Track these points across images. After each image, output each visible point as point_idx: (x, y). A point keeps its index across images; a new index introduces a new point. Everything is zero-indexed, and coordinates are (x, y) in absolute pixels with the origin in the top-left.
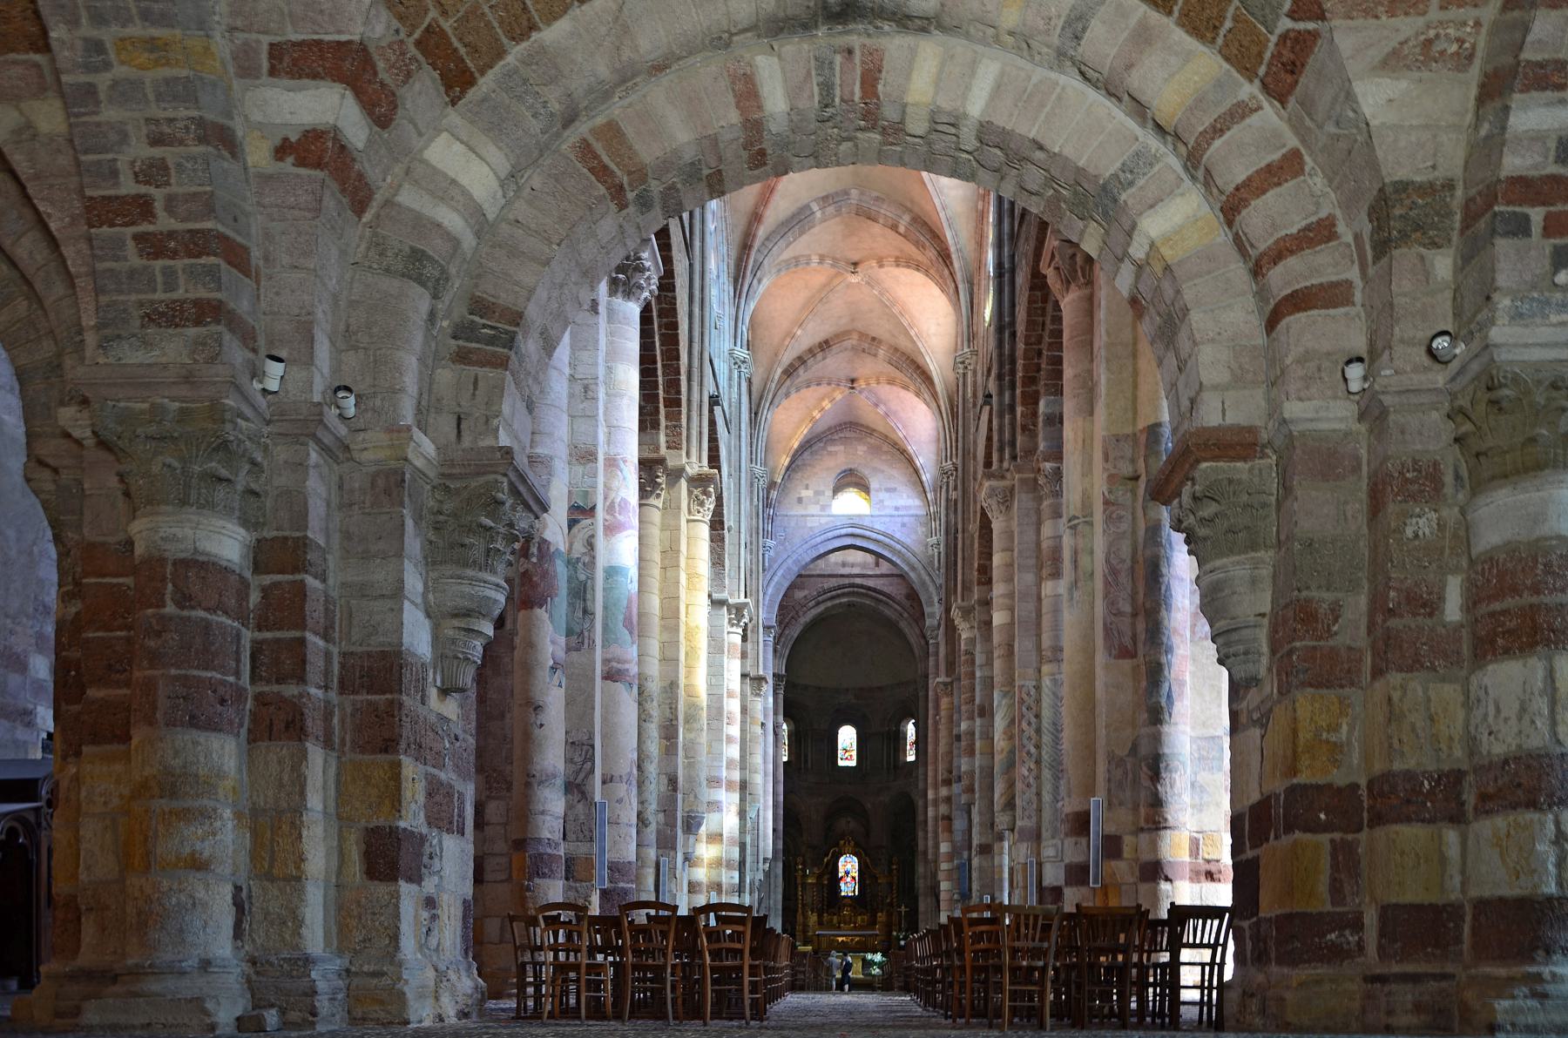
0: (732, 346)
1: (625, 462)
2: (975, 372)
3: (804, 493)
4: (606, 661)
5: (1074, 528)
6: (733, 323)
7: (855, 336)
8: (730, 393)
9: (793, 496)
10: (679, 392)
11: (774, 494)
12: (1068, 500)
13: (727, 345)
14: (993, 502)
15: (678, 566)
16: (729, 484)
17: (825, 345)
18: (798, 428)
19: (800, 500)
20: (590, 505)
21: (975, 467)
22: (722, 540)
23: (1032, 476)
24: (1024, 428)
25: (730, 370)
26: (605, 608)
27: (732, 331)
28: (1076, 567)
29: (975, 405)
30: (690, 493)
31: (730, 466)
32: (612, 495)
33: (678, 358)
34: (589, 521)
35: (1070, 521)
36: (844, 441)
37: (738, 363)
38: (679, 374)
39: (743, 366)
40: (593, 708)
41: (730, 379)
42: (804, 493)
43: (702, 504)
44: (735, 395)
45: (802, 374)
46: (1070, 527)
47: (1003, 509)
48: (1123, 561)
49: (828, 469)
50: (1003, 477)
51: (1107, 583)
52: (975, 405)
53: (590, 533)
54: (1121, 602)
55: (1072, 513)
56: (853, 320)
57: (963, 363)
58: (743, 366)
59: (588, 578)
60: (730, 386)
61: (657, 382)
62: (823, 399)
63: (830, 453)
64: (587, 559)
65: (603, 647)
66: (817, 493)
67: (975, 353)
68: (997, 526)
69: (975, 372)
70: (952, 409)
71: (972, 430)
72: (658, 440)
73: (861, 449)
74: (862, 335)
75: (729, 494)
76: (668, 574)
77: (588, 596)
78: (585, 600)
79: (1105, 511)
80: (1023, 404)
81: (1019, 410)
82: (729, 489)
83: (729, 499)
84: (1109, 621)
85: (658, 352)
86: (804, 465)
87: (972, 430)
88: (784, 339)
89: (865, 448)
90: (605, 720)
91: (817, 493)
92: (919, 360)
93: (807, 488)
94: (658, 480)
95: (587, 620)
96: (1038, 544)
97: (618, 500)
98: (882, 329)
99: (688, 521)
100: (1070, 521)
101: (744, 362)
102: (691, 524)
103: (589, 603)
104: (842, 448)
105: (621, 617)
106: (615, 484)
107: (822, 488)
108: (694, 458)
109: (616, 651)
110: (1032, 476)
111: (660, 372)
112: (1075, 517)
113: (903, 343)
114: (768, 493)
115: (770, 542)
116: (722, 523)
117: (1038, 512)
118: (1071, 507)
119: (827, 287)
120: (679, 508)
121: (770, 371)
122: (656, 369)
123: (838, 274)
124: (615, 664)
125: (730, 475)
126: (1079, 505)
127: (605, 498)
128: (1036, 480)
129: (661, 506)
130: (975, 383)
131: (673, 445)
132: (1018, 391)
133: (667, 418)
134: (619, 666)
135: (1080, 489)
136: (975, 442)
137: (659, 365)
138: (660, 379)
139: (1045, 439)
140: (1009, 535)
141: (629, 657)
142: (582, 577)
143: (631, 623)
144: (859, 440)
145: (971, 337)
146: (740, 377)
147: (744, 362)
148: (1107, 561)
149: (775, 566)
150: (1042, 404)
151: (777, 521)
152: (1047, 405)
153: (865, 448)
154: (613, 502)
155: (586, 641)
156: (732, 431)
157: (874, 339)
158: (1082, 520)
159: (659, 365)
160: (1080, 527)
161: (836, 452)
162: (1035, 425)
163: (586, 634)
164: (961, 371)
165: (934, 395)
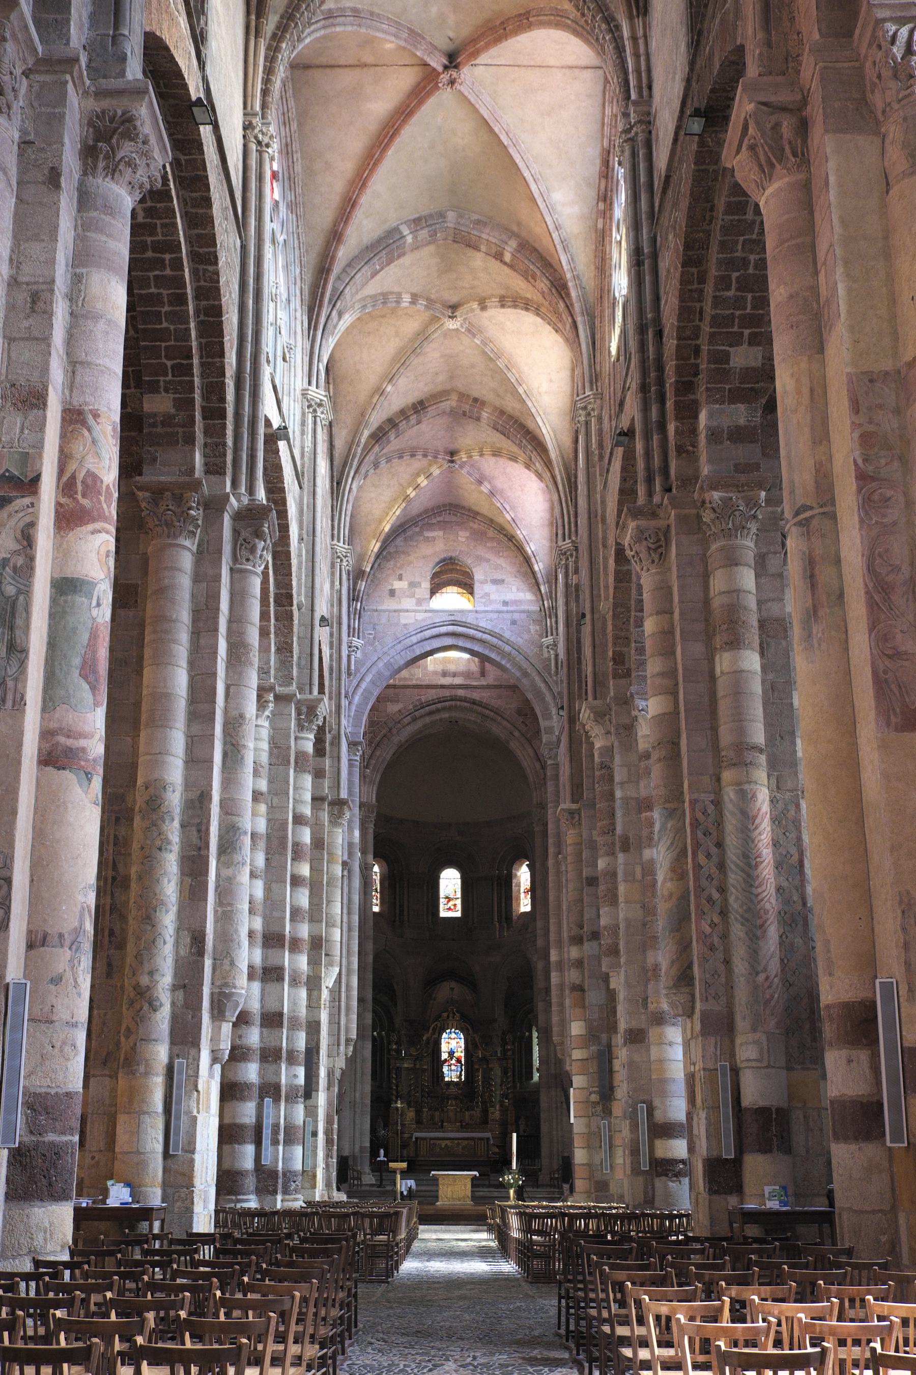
0: (306, 386)
1: (96, 416)
2: (600, 419)
3: (397, 585)
4: (46, 734)
5: (805, 524)
6: (307, 359)
7: (454, 397)
8: (302, 441)
10: (223, 400)
11: (362, 585)
12: (792, 482)
13: (300, 382)
14: (642, 548)
15: (216, 630)
16: (300, 550)
17: (419, 407)
18: (390, 508)
19: (392, 593)
20: (31, 475)
21: (604, 532)
22: (290, 617)
23: (694, 511)
24: (680, 450)
25: (303, 414)
26: (52, 644)
27: (306, 368)
28: (813, 586)
29: (601, 458)
30: (236, 532)
31: (301, 528)
32: (72, 467)
33: (222, 354)
34: (27, 501)
35: (797, 514)
36: (444, 525)
37: (312, 406)
38: (223, 375)
39: (319, 410)
40: (14, 812)
41: (303, 423)
42: (397, 585)
43: (253, 550)
44: (309, 443)
45: (394, 443)
46: (799, 524)
47: (656, 557)
48: (897, 569)
50: (654, 515)
51: (872, 606)
52: (601, 458)
53: (28, 519)
54: (899, 636)
55: (800, 501)
56: (452, 378)
57: (585, 408)
58: (319, 410)
59: (19, 592)
60: (303, 433)
61: (192, 382)
62: (418, 475)
64: (20, 561)
65: (44, 709)
66: (412, 585)
67: (600, 396)
68: (647, 580)
69: (600, 419)
70: (569, 480)
71: (599, 488)
72: (193, 459)
73: (463, 535)
74: (463, 396)
75: (300, 563)
76: (202, 642)
77: (19, 622)
78: (12, 628)
79: (859, 490)
80: (677, 418)
81: (671, 428)
82: (300, 555)
83: (300, 568)
84: (881, 667)
85: (194, 344)
86: (396, 552)
87: (599, 488)
88: (372, 396)
89: (467, 534)
90: (40, 834)
91: (412, 585)
92: (530, 425)
93: (400, 578)
94: (192, 512)
95: (15, 663)
96: (707, 602)
97: (81, 476)
98: (483, 389)
99: (231, 569)
100: (797, 514)
101: (320, 405)
102: (236, 576)
103: (18, 632)
104: (441, 533)
105: (77, 661)
106: (78, 448)
107: (417, 579)
108: (243, 490)
109: (65, 716)
110: (694, 511)
111: (196, 371)
112: (805, 508)
113: (510, 405)
114: (355, 584)
115: (357, 642)
116: (290, 596)
117: (704, 559)
118: (799, 492)
119: (422, 337)
120: (220, 552)
121: (355, 433)
122: (192, 365)
123: (435, 319)
124: (62, 739)
125: (301, 539)
126: (811, 487)
127: (61, 471)
128: (699, 517)
129: (194, 548)
130: (600, 432)
131: (215, 468)
132: (669, 404)
133: (207, 432)
134: (70, 742)
135: (811, 462)
136: (603, 502)
137: (196, 361)
138: (197, 380)
139: (710, 461)
140: (664, 590)
141: (87, 728)
142: (10, 590)
143: (95, 672)
145: (595, 378)
146: (315, 423)
147: (320, 405)
148: (870, 568)
149: (363, 670)
150: (703, 417)
151: (366, 616)
152: (711, 416)
153: (467, 534)
154: (73, 478)
155: (10, 697)
156: (305, 486)
157: (476, 400)
158: (816, 511)
159: (196, 361)
160: (815, 522)
162: (694, 445)
163: (10, 684)
164: (583, 419)
165: (548, 464)
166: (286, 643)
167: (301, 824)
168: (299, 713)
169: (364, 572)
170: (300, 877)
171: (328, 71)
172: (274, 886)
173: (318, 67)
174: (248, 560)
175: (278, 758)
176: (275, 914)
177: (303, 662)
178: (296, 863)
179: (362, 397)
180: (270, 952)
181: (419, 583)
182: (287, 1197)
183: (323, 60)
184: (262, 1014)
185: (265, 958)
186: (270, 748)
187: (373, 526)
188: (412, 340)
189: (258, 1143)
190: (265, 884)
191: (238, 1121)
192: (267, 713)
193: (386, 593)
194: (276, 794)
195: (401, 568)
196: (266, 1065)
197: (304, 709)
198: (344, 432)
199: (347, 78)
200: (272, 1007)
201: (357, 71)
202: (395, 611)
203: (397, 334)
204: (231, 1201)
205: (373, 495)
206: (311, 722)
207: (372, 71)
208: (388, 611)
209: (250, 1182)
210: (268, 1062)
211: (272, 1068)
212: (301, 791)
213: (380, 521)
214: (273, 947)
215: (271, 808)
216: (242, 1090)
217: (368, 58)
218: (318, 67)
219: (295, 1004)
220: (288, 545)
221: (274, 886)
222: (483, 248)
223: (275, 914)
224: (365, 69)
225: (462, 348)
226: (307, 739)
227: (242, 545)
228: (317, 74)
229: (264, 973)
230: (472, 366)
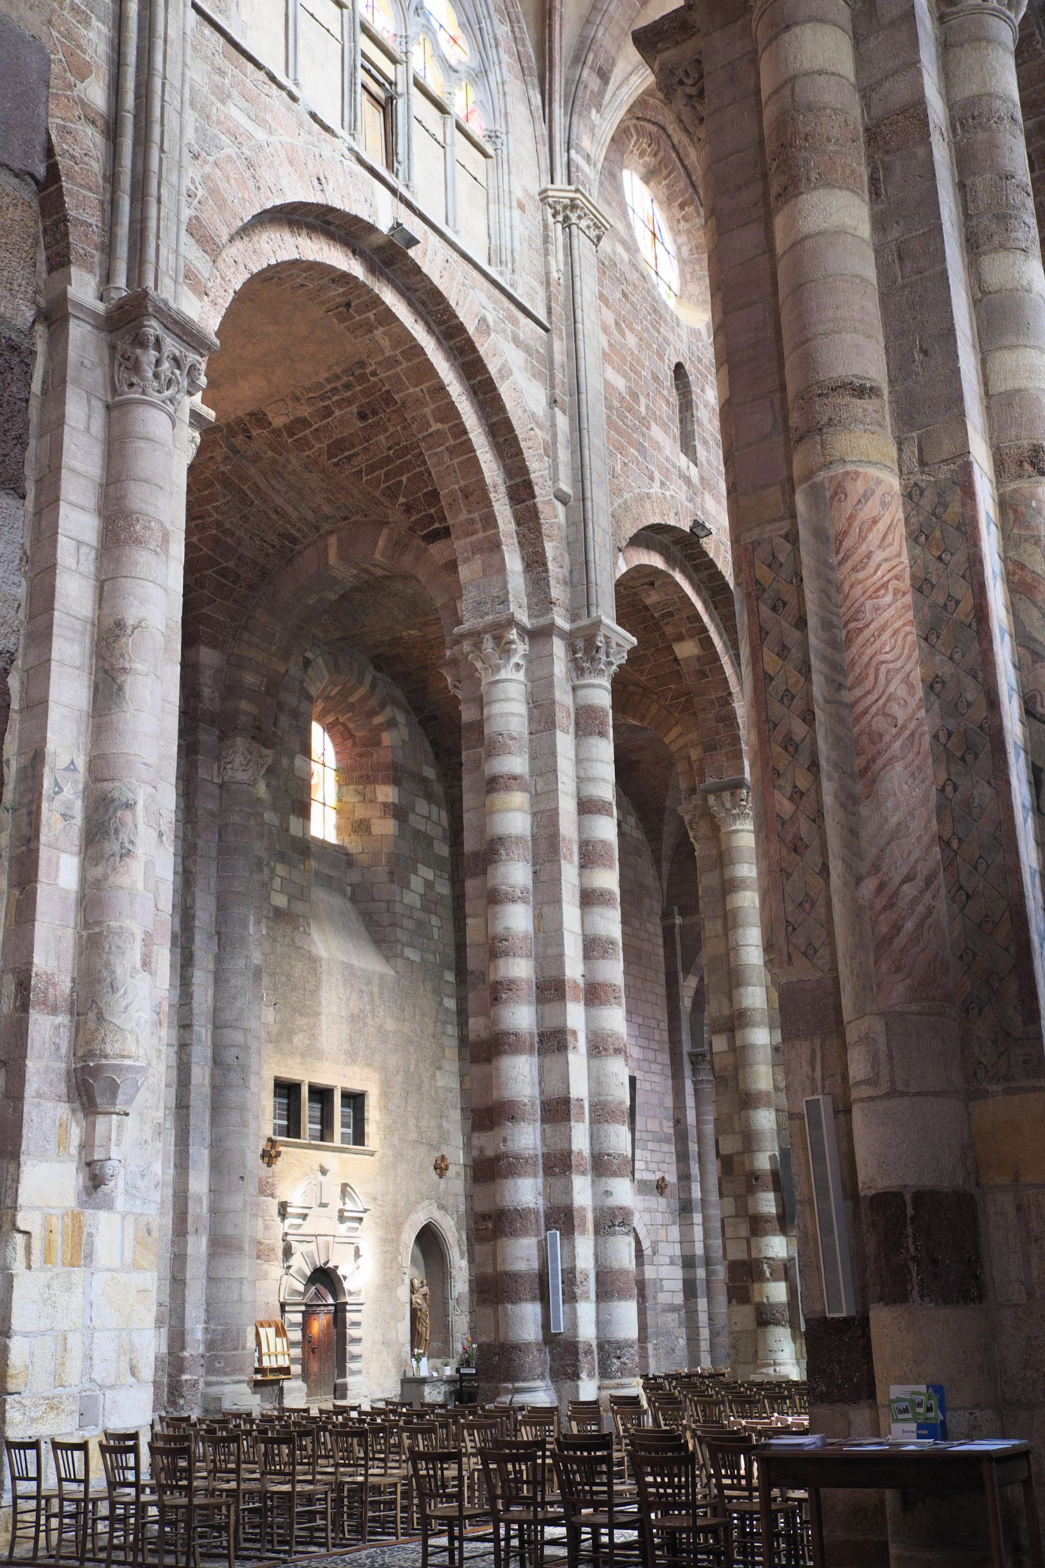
25: (546, 227)
41: (546, 239)
44: (557, 264)
101: (573, 207)
116: (528, 485)
166: (536, 553)
167: (591, 812)
168: (572, 649)
170: (594, 891)
172: (546, 910)
174: (131, 385)
175: (539, 721)
176: (551, 951)
177: (576, 576)
178: (587, 872)
180: (547, 1007)
182: (607, 1382)
184: (542, 1103)
185: (540, 1019)
186: (530, 710)
189: (544, 1298)
190: (535, 909)
191: (509, 1268)
192: (516, 659)
194: (541, 775)
196: (552, 1180)
197: (580, 644)
200: (555, 1090)
204: (508, 1391)
206: (593, 660)
209: (537, 1360)
210: (553, 1174)
211: (559, 1183)
212: (586, 764)
214: (550, 1001)
215: (536, 797)
216: (513, 1220)
219: (599, 1083)
220: (503, 409)
221: (546, 910)
223: (551, 951)
226: (600, 686)
227: (120, 365)
229: (541, 1041)
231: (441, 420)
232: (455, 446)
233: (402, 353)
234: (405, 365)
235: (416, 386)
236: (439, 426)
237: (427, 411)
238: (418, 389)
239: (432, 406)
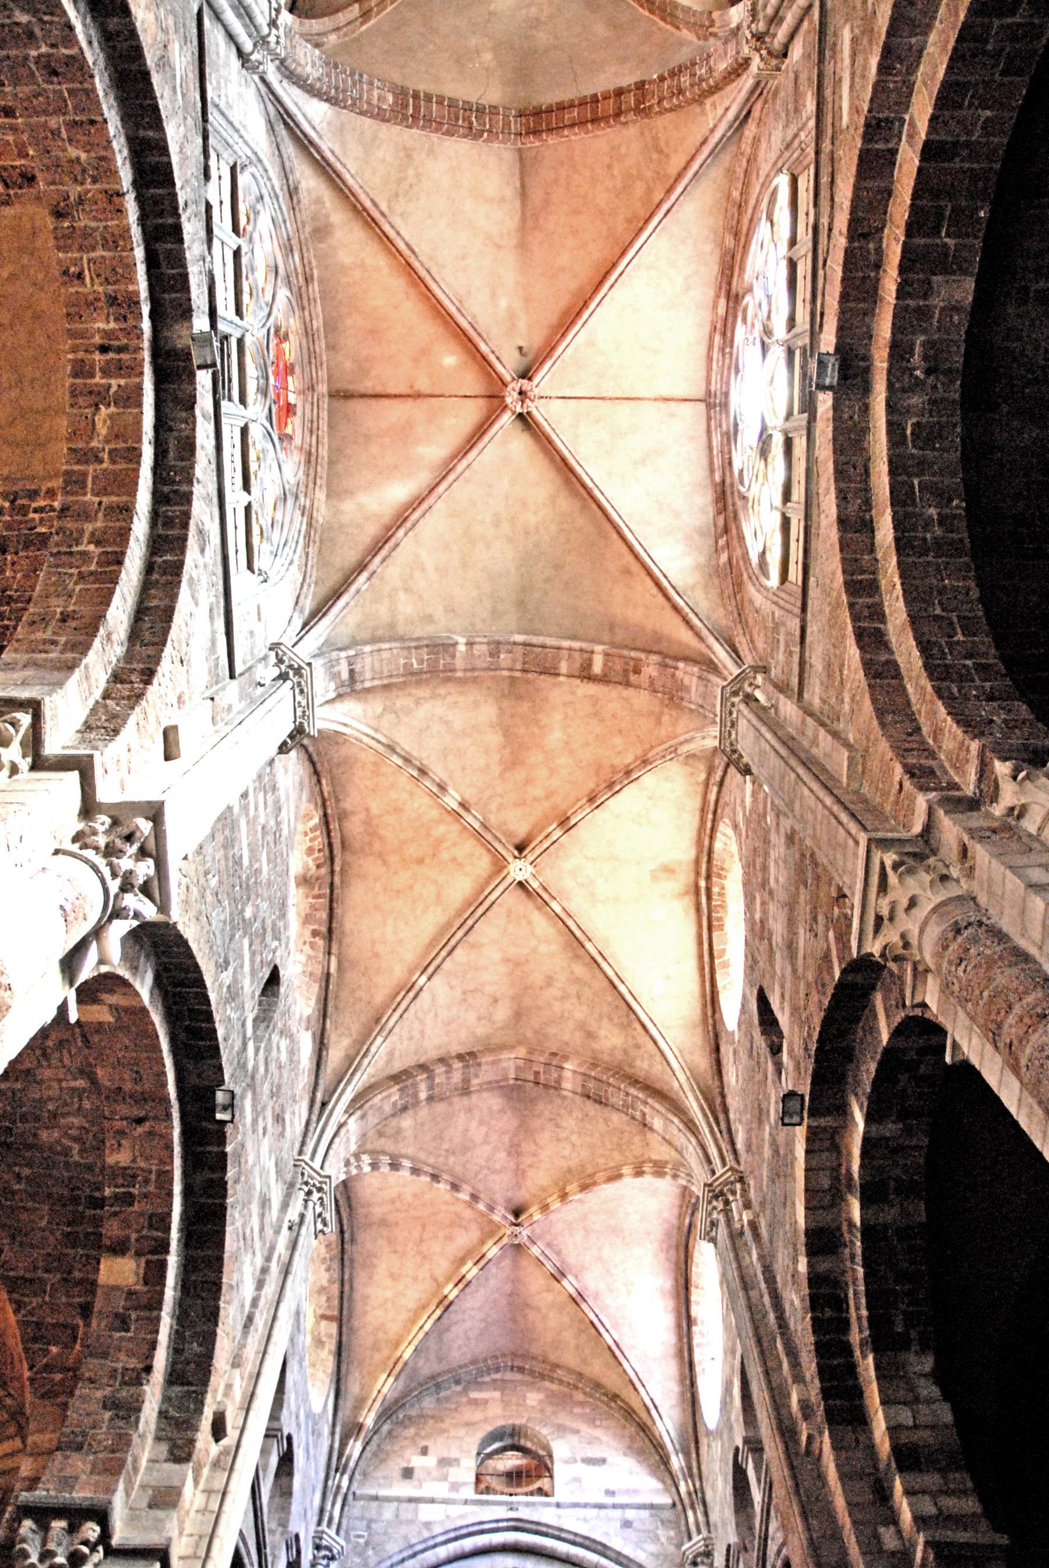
3: (417, 1461)
9: (396, 1465)
18: (413, 1322)
19: (408, 1473)
36: (501, 1386)
42: (417, 1461)
49: (468, 1424)
62: (462, 1261)
63: (475, 1402)
66: (444, 1462)
86: (421, 1416)
93: (424, 1451)
107: (454, 1454)
114: (343, 1445)
144: (531, 1385)
161: (486, 1402)
169: (361, 1426)
171: (373, 402)
173: (363, 396)
179: (379, 997)
181: (457, 1461)
183: (368, 385)
187: (386, 1352)
188: (459, 913)
193: (397, 1473)
195: (427, 1437)
198: (346, 1042)
199: (395, 412)
201: (409, 403)
202: (410, 1500)
203: (439, 899)
205: (388, 1294)
207: (424, 404)
208: (398, 1499)
213: (397, 1344)
217: (423, 385)
218: (363, 396)
222: (564, 667)
224: (419, 401)
225: (533, 943)
228: (357, 406)
230: (549, 981)
231: (98, 543)
232: (92, 573)
233: (111, 452)
234: (105, 465)
235: (97, 495)
236: (92, 548)
237: (89, 527)
238: (97, 499)
239: (99, 524)
